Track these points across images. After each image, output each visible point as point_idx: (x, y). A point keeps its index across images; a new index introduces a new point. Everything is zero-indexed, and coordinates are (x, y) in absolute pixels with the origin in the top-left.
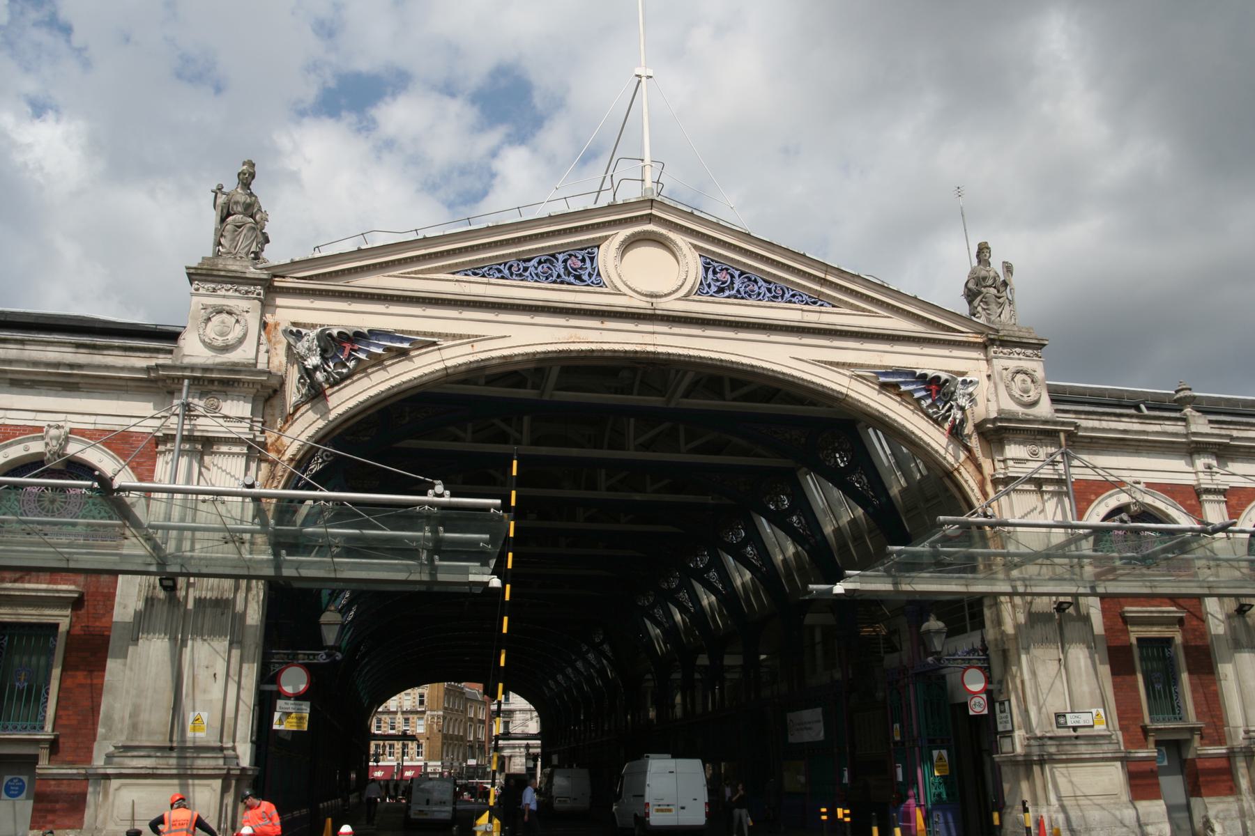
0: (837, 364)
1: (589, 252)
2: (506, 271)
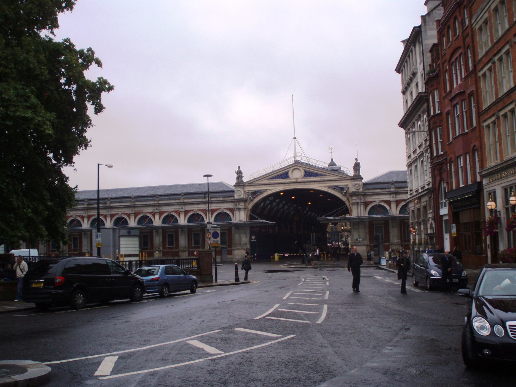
0: (326, 186)
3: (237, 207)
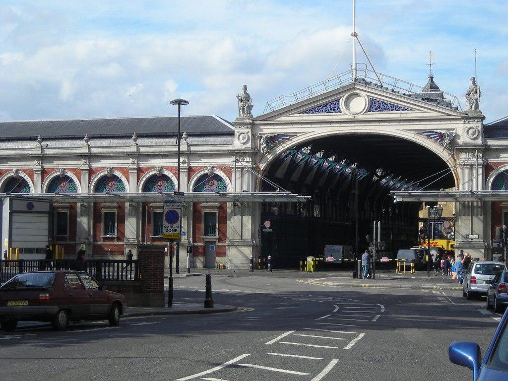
1: (337, 101)
2: (314, 111)
3: (239, 165)
